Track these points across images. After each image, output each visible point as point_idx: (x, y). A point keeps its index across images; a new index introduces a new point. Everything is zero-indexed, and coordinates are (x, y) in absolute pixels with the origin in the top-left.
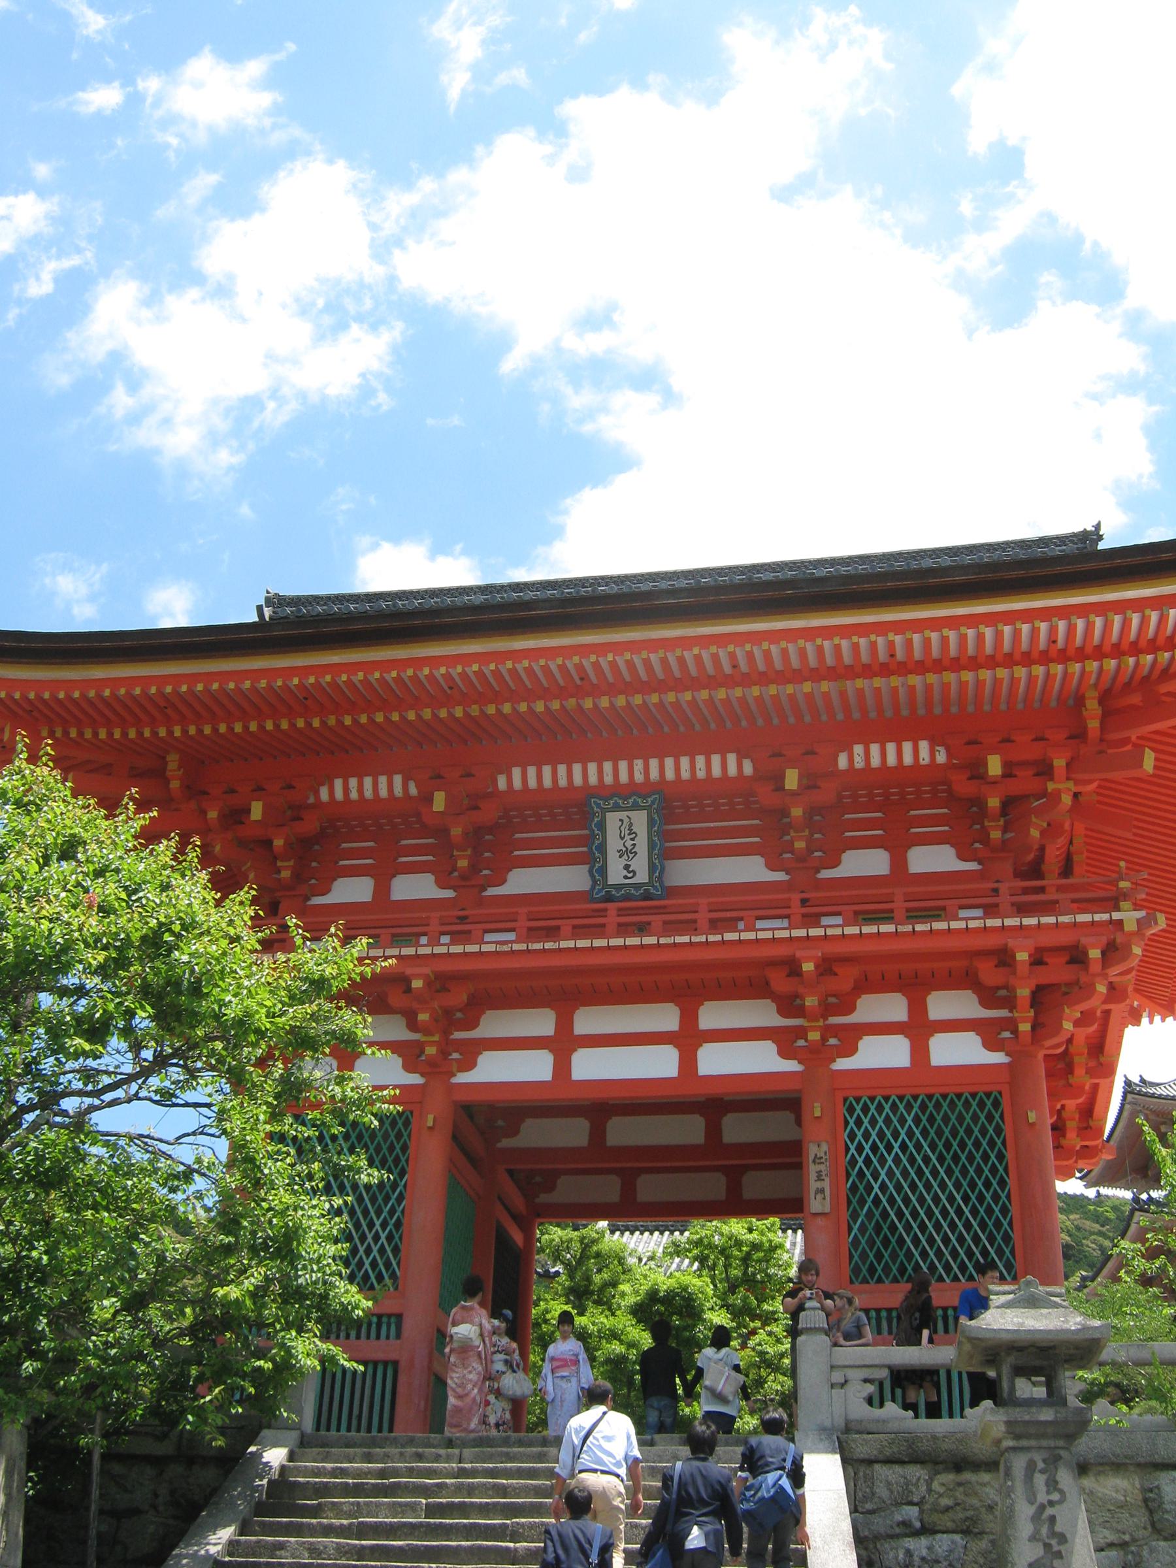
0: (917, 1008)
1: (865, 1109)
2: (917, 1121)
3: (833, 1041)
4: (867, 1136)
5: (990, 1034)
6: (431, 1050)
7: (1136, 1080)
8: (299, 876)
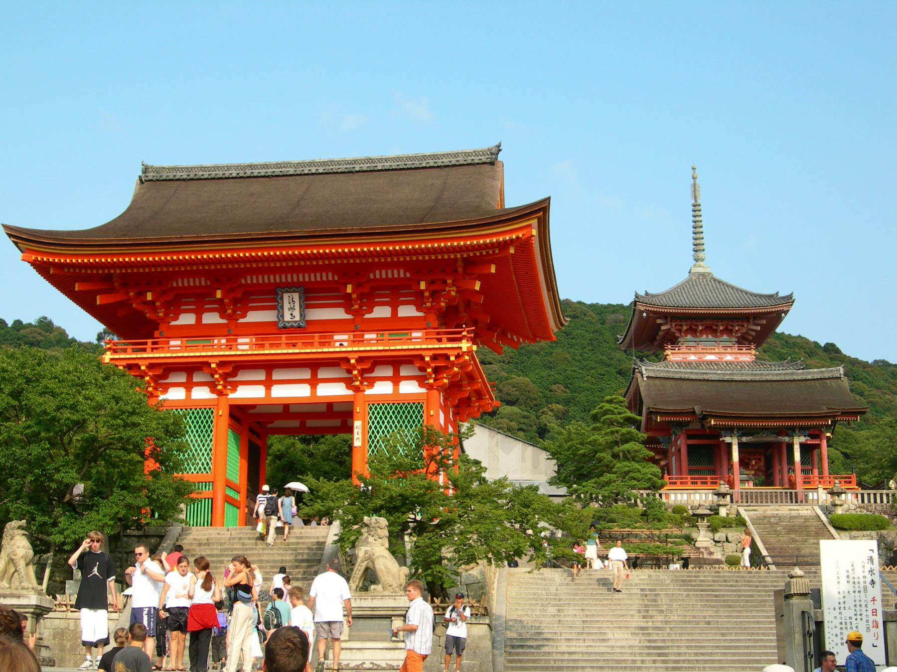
0: (396, 371)
1: (376, 408)
2: (394, 413)
3: (365, 383)
4: (376, 418)
5: (421, 381)
6: (220, 387)
7: (642, 293)
8: (166, 314)
